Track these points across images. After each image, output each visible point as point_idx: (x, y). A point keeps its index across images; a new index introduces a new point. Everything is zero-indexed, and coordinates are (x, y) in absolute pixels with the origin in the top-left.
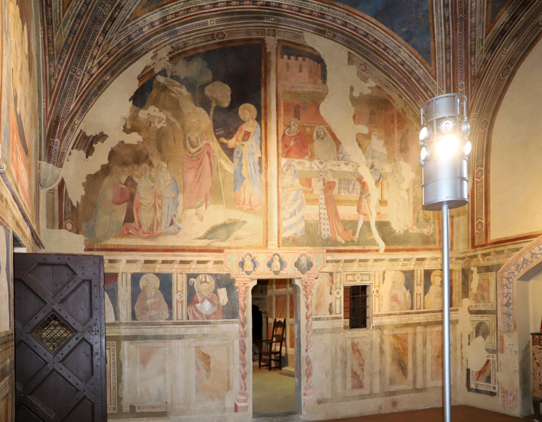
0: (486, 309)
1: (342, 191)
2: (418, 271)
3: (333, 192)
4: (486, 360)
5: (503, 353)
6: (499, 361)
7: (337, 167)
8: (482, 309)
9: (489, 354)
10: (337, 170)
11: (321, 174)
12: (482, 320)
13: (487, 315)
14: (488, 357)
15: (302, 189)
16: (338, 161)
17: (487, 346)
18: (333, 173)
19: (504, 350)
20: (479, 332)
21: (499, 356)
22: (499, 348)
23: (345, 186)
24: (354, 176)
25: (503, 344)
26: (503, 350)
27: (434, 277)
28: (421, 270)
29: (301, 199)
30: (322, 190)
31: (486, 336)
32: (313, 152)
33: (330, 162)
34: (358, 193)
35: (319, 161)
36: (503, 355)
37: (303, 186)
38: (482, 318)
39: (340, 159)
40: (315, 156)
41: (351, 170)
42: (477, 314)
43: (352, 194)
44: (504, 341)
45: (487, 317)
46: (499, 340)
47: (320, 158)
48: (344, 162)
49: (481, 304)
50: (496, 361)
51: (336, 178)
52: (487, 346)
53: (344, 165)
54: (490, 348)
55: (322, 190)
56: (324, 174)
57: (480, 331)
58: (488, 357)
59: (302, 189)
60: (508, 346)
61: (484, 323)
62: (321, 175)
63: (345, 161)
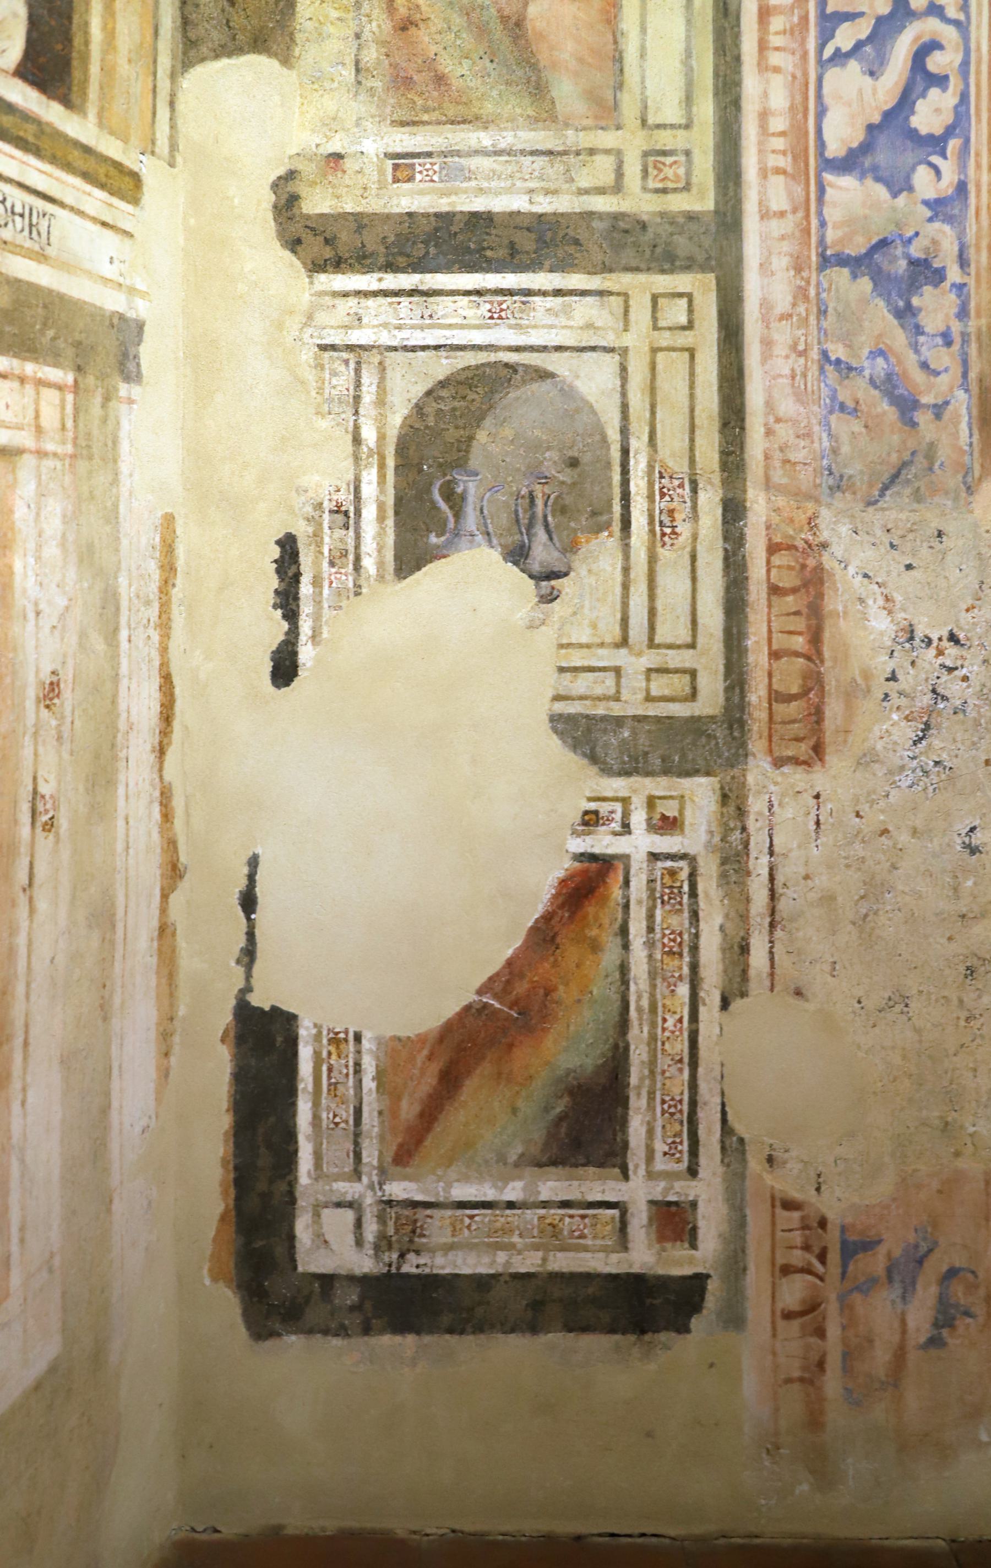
0: (564, 204)
4: (561, 868)
5: (818, 750)
6: (760, 865)
8: (499, 204)
9: (617, 786)
12: (504, 335)
13: (576, 280)
14: (591, 820)
17: (582, 684)
19: (833, 710)
20: (455, 500)
21: (756, 805)
22: (757, 695)
25: (816, 638)
26: (817, 714)
31: (571, 548)
36: (819, 779)
38: (496, 317)
42: (418, 266)
44: (833, 603)
45: (585, 309)
46: (757, 592)
49: (485, 139)
50: (709, 869)
52: (582, 684)
54: (632, 704)
57: (471, 487)
58: (591, 820)
60: (884, 665)
61: (544, 375)
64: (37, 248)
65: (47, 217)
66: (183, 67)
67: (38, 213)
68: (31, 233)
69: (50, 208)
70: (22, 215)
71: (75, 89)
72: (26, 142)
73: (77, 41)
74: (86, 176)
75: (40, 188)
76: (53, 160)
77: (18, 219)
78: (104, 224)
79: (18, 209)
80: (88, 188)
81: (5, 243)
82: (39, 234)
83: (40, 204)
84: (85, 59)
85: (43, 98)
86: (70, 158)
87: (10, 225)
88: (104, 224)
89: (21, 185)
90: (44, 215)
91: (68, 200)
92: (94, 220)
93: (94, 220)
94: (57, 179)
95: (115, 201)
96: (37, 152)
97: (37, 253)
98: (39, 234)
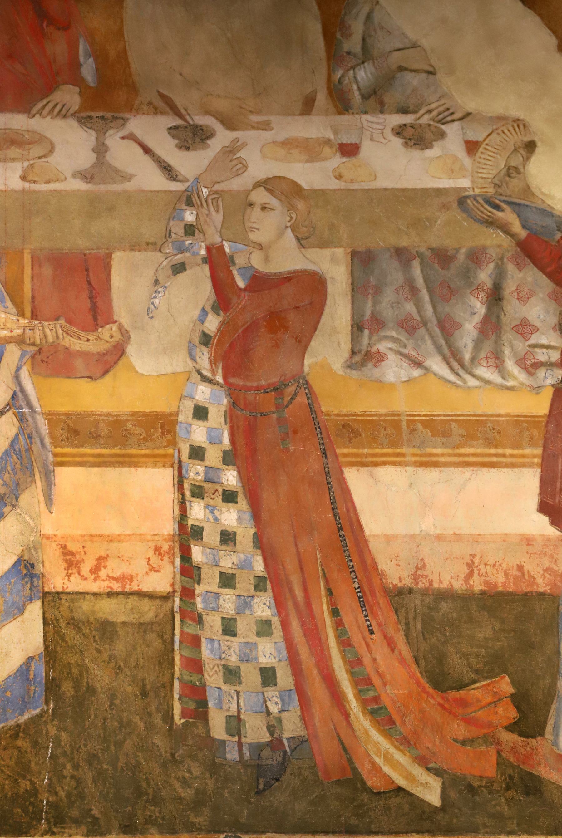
1: (383, 346)
3: (307, 361)
7: (337, 161)
10: (334, 184)
11: (189, 217)
15: (20, 341)
16: (345, 119)
18: (301, 205)
23: (410, 307)
24: (490, 223)
29: (9, 416)
30: (206, 339)
32: (123, 55)
33: (266, 126)
34: (541, 356)
35: (173, 121)
37: (34, 316)
39: (357, 97)
40: (133, 89)
41: (465, 183)
43: (483, 372)
47: (179, 102)
48: (398, 119)
51: (323, 245)
53: (397, 142)
55: (206, 339)
56: (218, 218)
59: (20, 341)
62: (190, 230)
63: (404, 111)
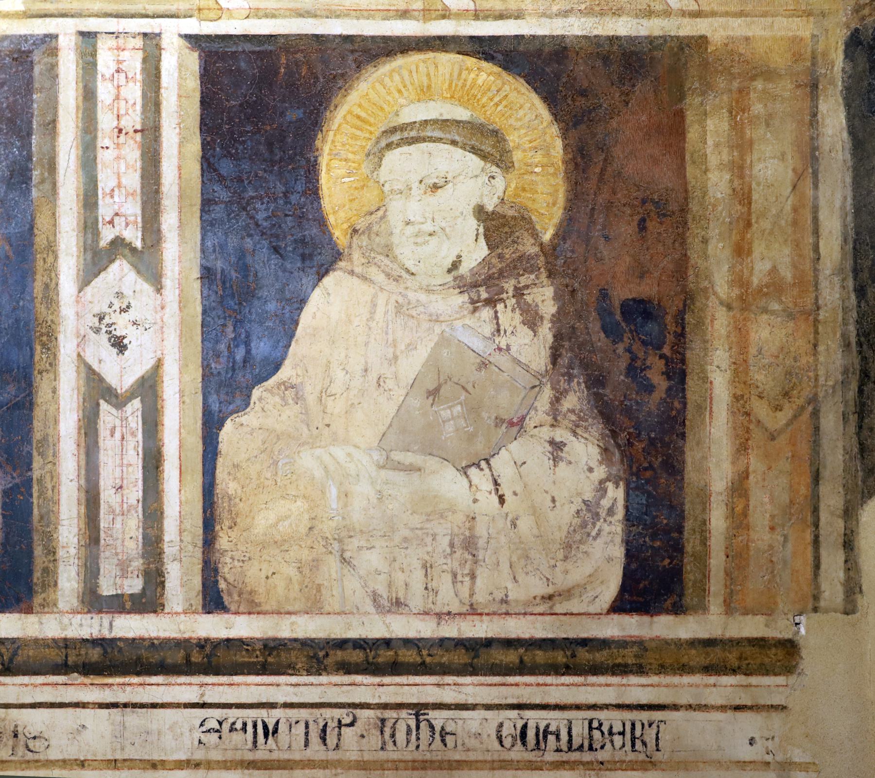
2: (105, 60)
27: (377, 155)
28: (151, 40)
64: (642, 757)
65: (654, 726)
66: (862, 498)
67: (643, 725)
68: (633, 745)
69: (657, 715)
70: (622, 733)
71: (689, 591)
72: (626, 665)
73: (691, 544)
74: (708, 669)
75: (644, 701)
76: (662, 669)
77: (618, 740)
78: (738, 708)
79: (617, 728)
80: (712, 680)
81: (602, 763)
82: (644, 744)
83: (645, 716)
84: (702, 558)
85: (646, 619)
86: (685, 660)
87: (608, 746)
88: (738, 708)
89: (619, 707)
90: (650, 725)
91: (683, 701)
92: (723, 708)
93: (723, 708)
94: (667, 686)
95: (754, 680)
96: (640, 670)
97: (643, 762)
98: (644, 744)
